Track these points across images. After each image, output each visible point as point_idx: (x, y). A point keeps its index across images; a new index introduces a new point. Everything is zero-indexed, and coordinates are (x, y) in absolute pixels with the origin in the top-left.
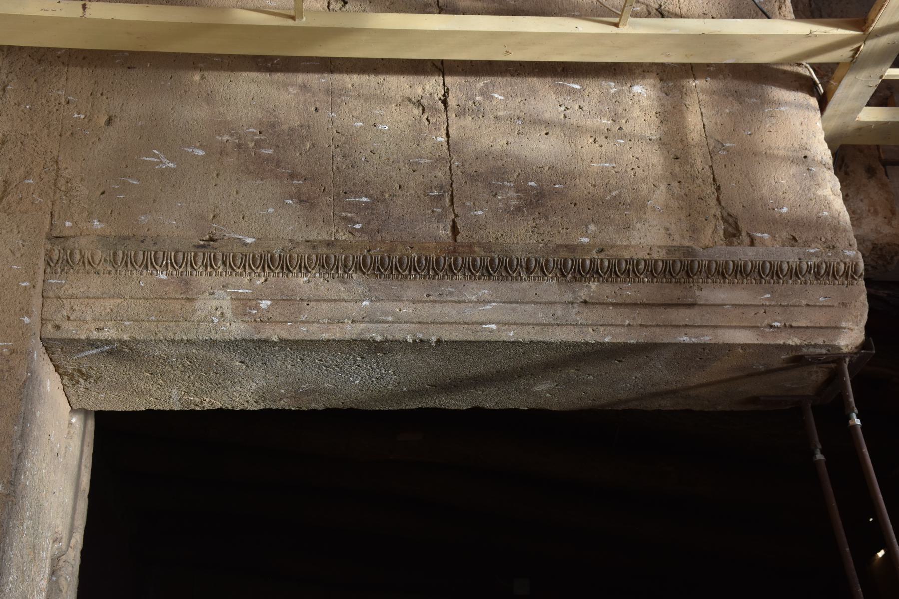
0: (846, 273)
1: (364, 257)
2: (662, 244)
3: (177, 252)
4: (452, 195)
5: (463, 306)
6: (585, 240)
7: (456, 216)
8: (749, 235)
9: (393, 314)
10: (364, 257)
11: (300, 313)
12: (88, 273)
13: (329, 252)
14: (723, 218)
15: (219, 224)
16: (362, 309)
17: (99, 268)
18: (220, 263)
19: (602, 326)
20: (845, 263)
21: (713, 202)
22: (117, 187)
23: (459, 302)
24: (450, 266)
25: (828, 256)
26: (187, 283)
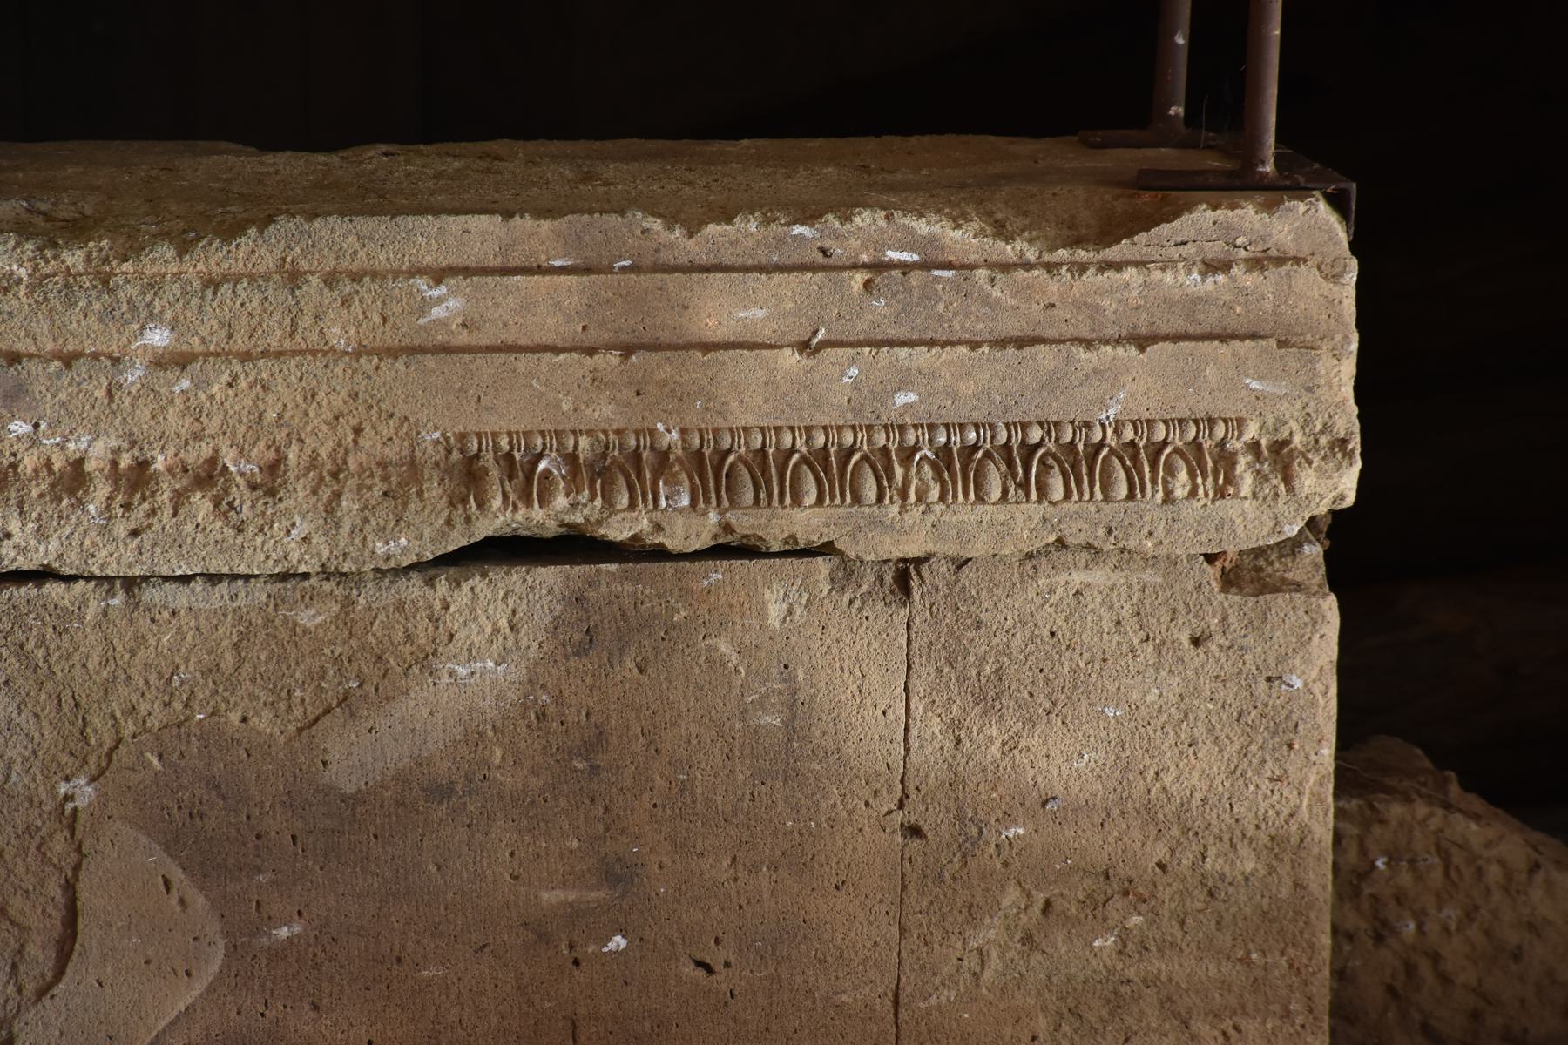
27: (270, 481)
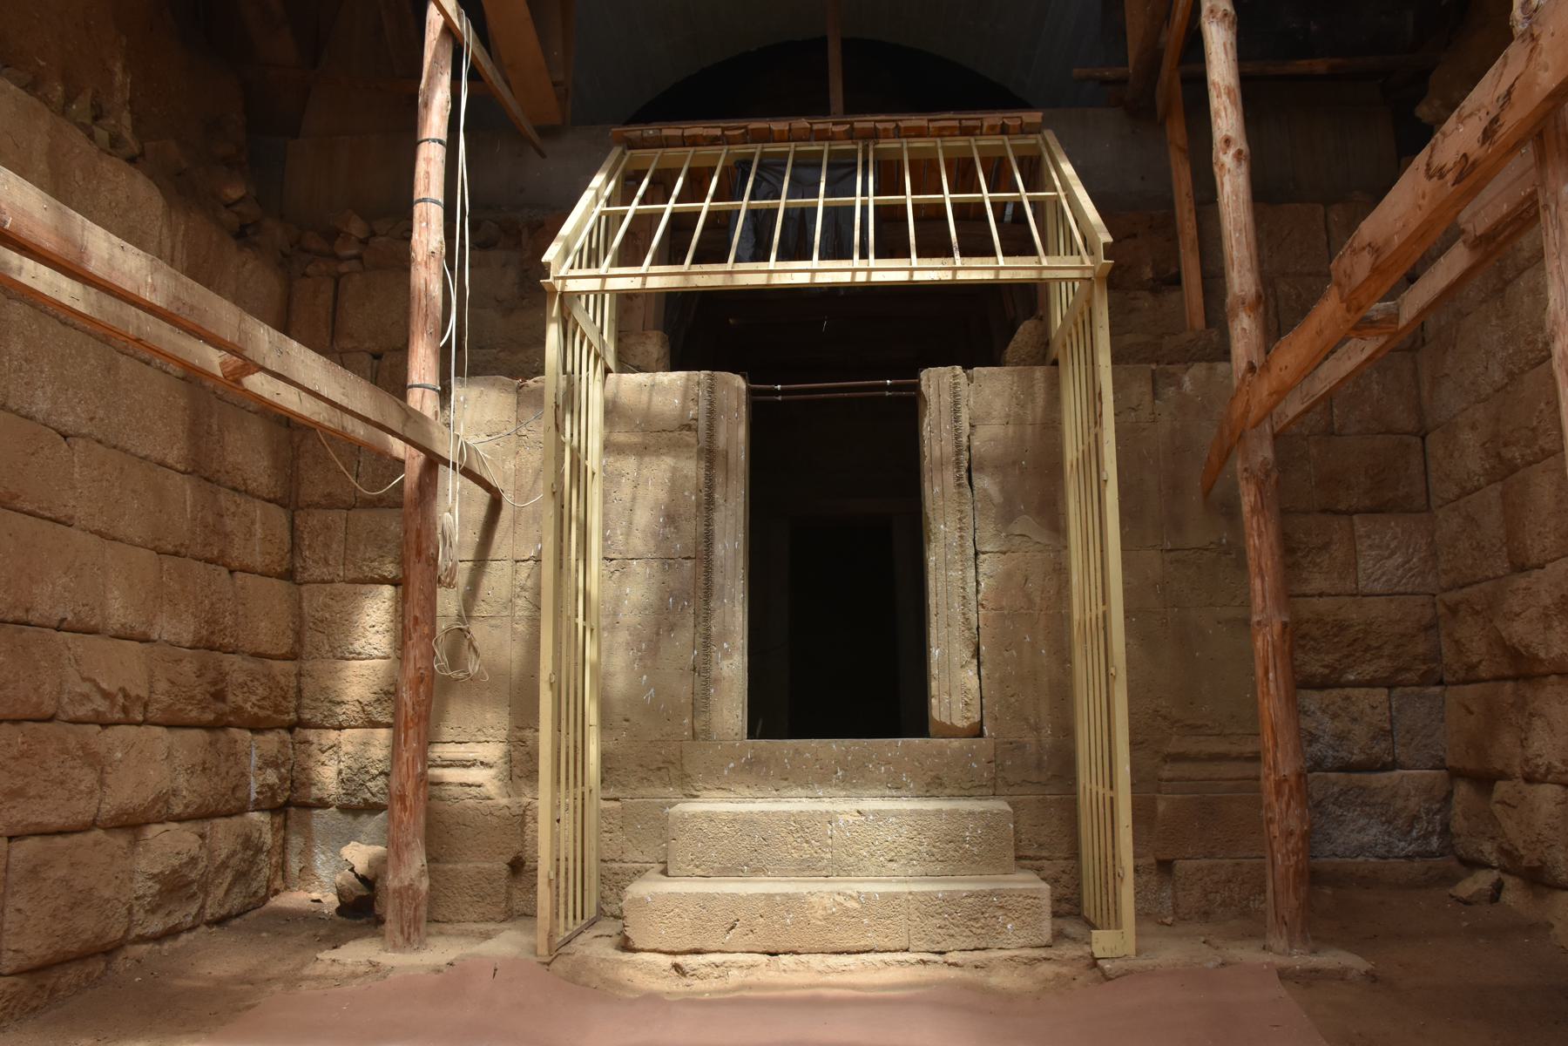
6: (693, 498)
21: (671, 434)
27: (961, 512)
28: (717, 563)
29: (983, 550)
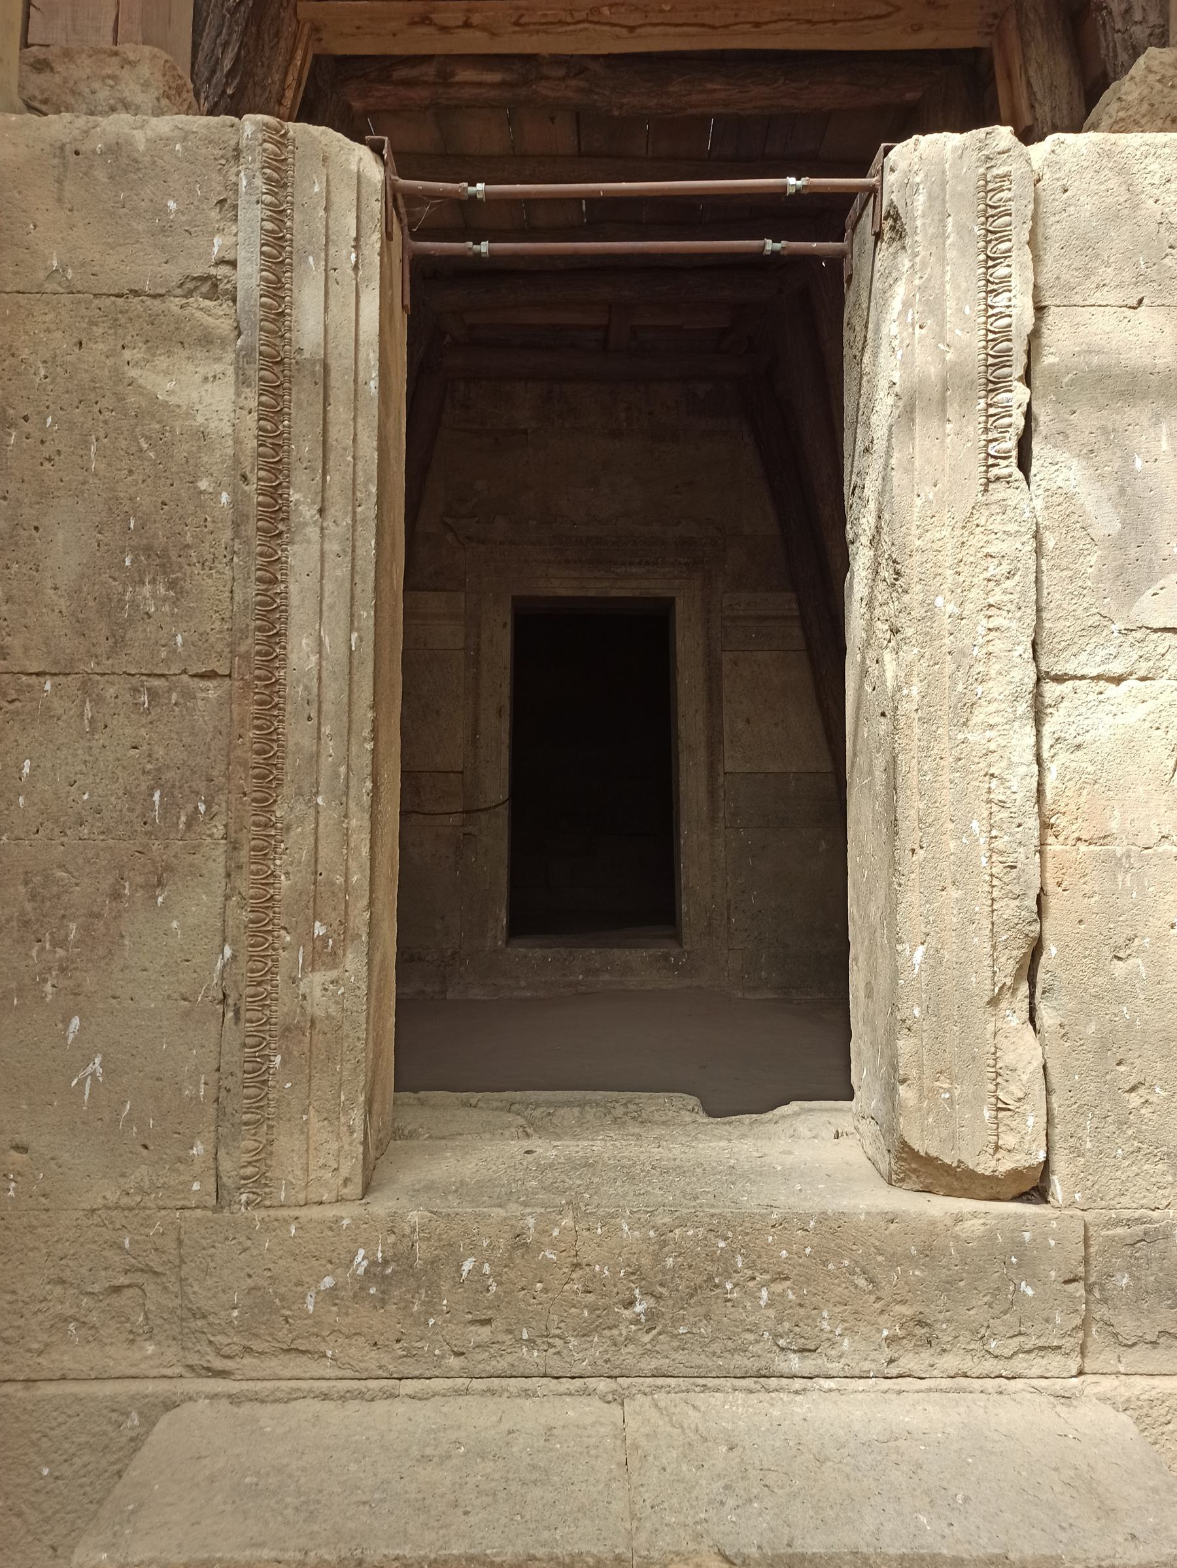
0: (277, 143)
1: (255, 800)
2: (232, 390)
3: (244, 1045)
4: (148, 675)
5: (324, 675)
6: (225, 498)
7: (185, 672)
8: (217, 264)
9: (335, 766)
10: (255, 800)
11: (333, 884)
12: (272, 1153)
13: (246, 848)
14: (185, 296)
15: (197, 993)
16: (329, 803)
17: (264, 1142)
18: (260, 989)
19: (354, 494)
20: (265, 141)
22: (135, 1129)
23: (320, 678)
24: (266, 686)
25: (254, 161)
26: (288, 1029)
28: (295, 693)
29: (1059, 669)
